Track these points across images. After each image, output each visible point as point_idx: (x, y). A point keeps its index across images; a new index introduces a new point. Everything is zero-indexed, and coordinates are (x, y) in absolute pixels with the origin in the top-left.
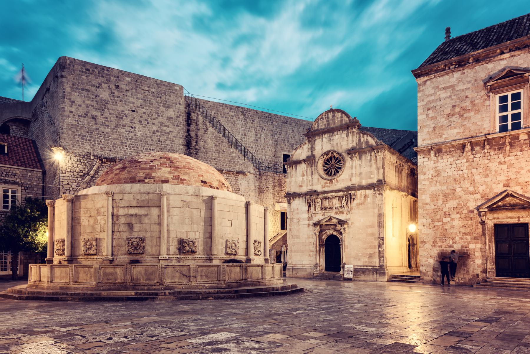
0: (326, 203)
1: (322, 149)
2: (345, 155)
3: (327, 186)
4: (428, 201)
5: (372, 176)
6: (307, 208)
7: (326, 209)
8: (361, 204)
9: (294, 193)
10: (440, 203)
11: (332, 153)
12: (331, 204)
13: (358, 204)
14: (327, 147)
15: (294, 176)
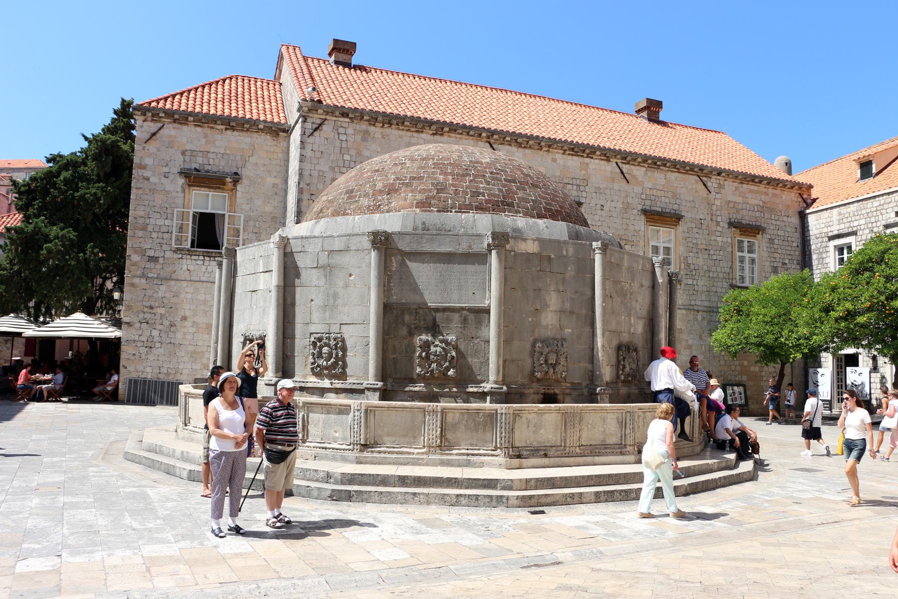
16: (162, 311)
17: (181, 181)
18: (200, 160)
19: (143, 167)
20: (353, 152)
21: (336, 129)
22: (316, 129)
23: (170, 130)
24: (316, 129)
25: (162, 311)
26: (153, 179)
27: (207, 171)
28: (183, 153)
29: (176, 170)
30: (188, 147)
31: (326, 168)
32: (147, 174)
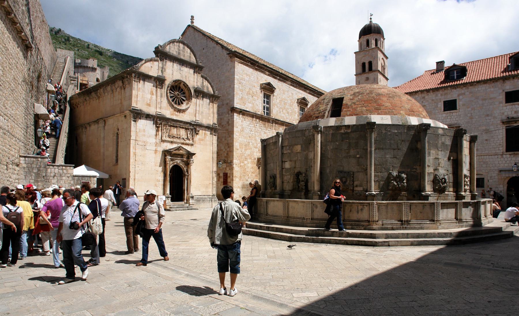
0: (174, 131)
1: (173, 74)
2: (192, 91)
3: (176, 115)
4: (238, 148)
5: (210, 118)
6: (154, 132)
7: (173, 137)
8: (202, 140)
9: (140, 110)
10: (243, 150)
11: (180, 83)
12: (179, 133)
13: (201, 140)
14: (177, 76)
15: (141, 90)
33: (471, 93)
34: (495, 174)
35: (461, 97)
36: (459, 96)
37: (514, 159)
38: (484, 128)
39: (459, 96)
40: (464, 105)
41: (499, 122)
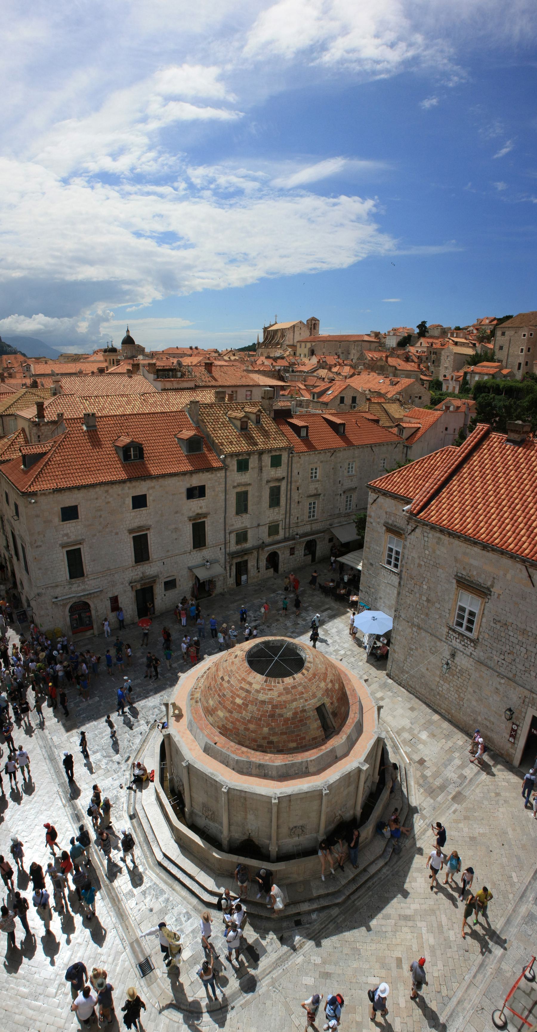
16: (373, 590)
17: (384, 528)
18: (393, 518)
19: (370, 517)
20: (430, 550)
21: (423, 532)
22: (413, 531)
23: (381, 500)
24: (413, 531)
25: (373, 590)
26: (374, 524)
27: (395, 526)
28: (386, 513)
29: (382, 522)
30: (388, 510)
31: (416, 556)
32: (372, 520)
33: (161, 486)
34: (185, 572)
35: (151, 491)
36: (148, 489)
37: (199, 554)
38: (173, 526)
39: (148, 489)
40: (154, 501)
41: (186, 519)
